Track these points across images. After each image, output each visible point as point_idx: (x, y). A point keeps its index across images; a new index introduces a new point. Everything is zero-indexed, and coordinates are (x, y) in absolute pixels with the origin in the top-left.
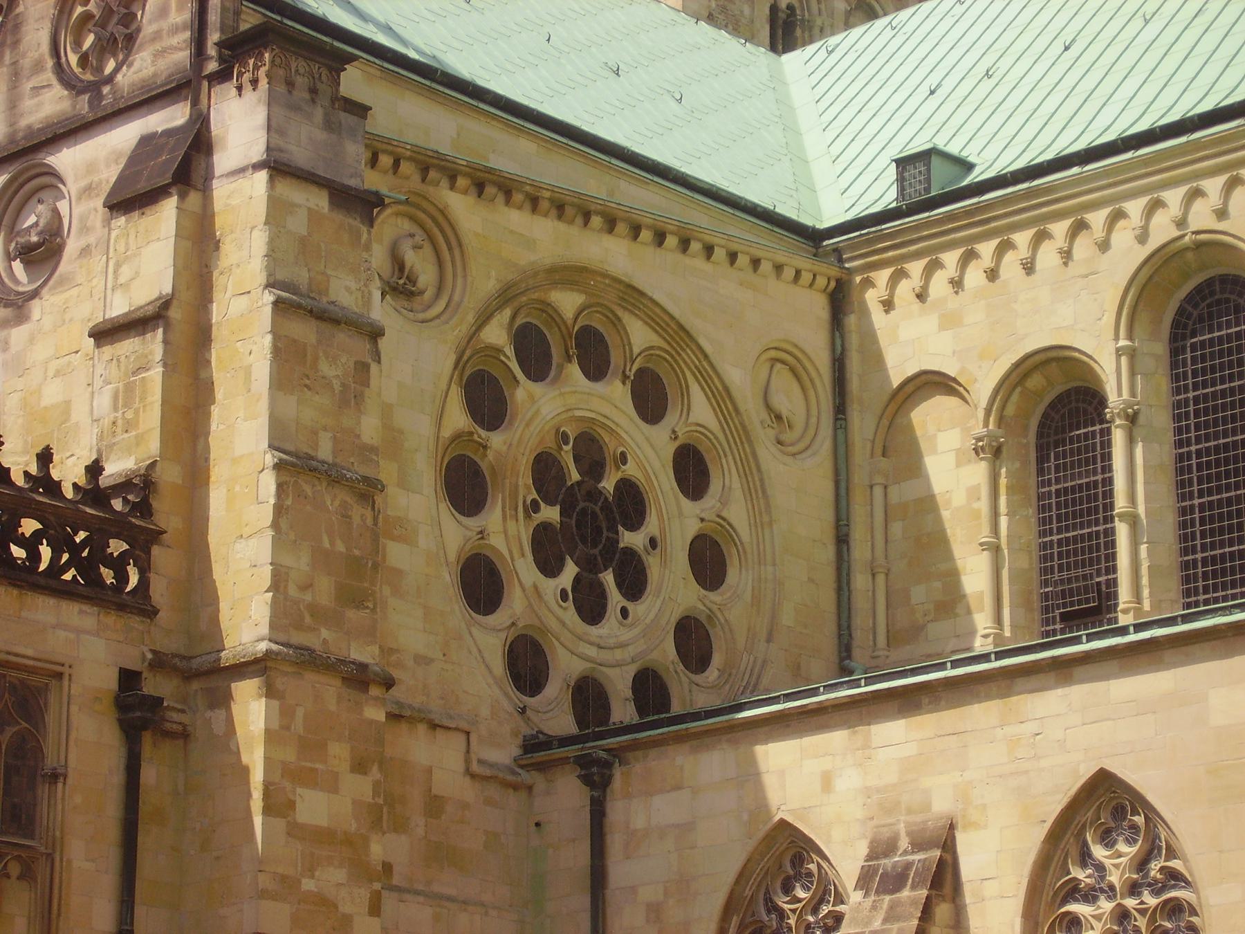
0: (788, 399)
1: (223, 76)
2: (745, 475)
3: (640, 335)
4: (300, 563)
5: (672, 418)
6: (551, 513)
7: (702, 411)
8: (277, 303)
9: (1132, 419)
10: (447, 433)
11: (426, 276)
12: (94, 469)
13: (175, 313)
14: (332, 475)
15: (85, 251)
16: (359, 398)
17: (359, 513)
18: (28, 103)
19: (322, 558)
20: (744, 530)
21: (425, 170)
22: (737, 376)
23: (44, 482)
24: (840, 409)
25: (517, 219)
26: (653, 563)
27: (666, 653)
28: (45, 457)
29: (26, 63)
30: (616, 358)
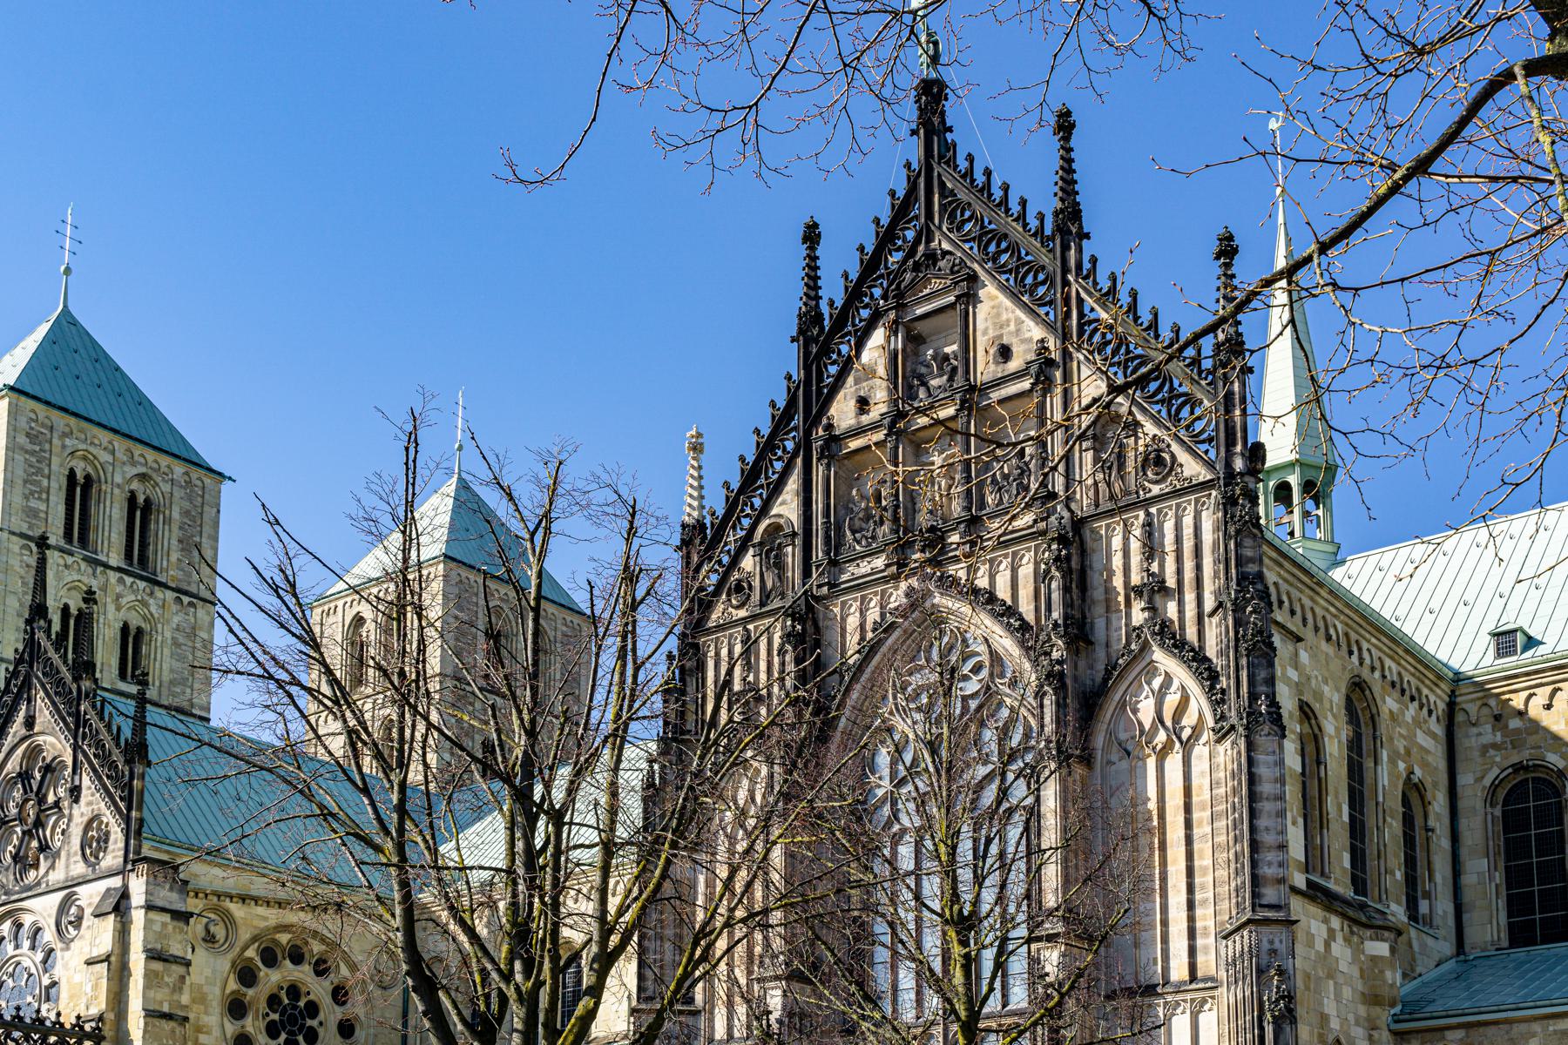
1: (133, 870)
10: (228, 991)
13: (113, 959)
15: (89, 927)
16: (181, 989)
18: (72, 867)
21: (219, 896)
29: (72, 851)
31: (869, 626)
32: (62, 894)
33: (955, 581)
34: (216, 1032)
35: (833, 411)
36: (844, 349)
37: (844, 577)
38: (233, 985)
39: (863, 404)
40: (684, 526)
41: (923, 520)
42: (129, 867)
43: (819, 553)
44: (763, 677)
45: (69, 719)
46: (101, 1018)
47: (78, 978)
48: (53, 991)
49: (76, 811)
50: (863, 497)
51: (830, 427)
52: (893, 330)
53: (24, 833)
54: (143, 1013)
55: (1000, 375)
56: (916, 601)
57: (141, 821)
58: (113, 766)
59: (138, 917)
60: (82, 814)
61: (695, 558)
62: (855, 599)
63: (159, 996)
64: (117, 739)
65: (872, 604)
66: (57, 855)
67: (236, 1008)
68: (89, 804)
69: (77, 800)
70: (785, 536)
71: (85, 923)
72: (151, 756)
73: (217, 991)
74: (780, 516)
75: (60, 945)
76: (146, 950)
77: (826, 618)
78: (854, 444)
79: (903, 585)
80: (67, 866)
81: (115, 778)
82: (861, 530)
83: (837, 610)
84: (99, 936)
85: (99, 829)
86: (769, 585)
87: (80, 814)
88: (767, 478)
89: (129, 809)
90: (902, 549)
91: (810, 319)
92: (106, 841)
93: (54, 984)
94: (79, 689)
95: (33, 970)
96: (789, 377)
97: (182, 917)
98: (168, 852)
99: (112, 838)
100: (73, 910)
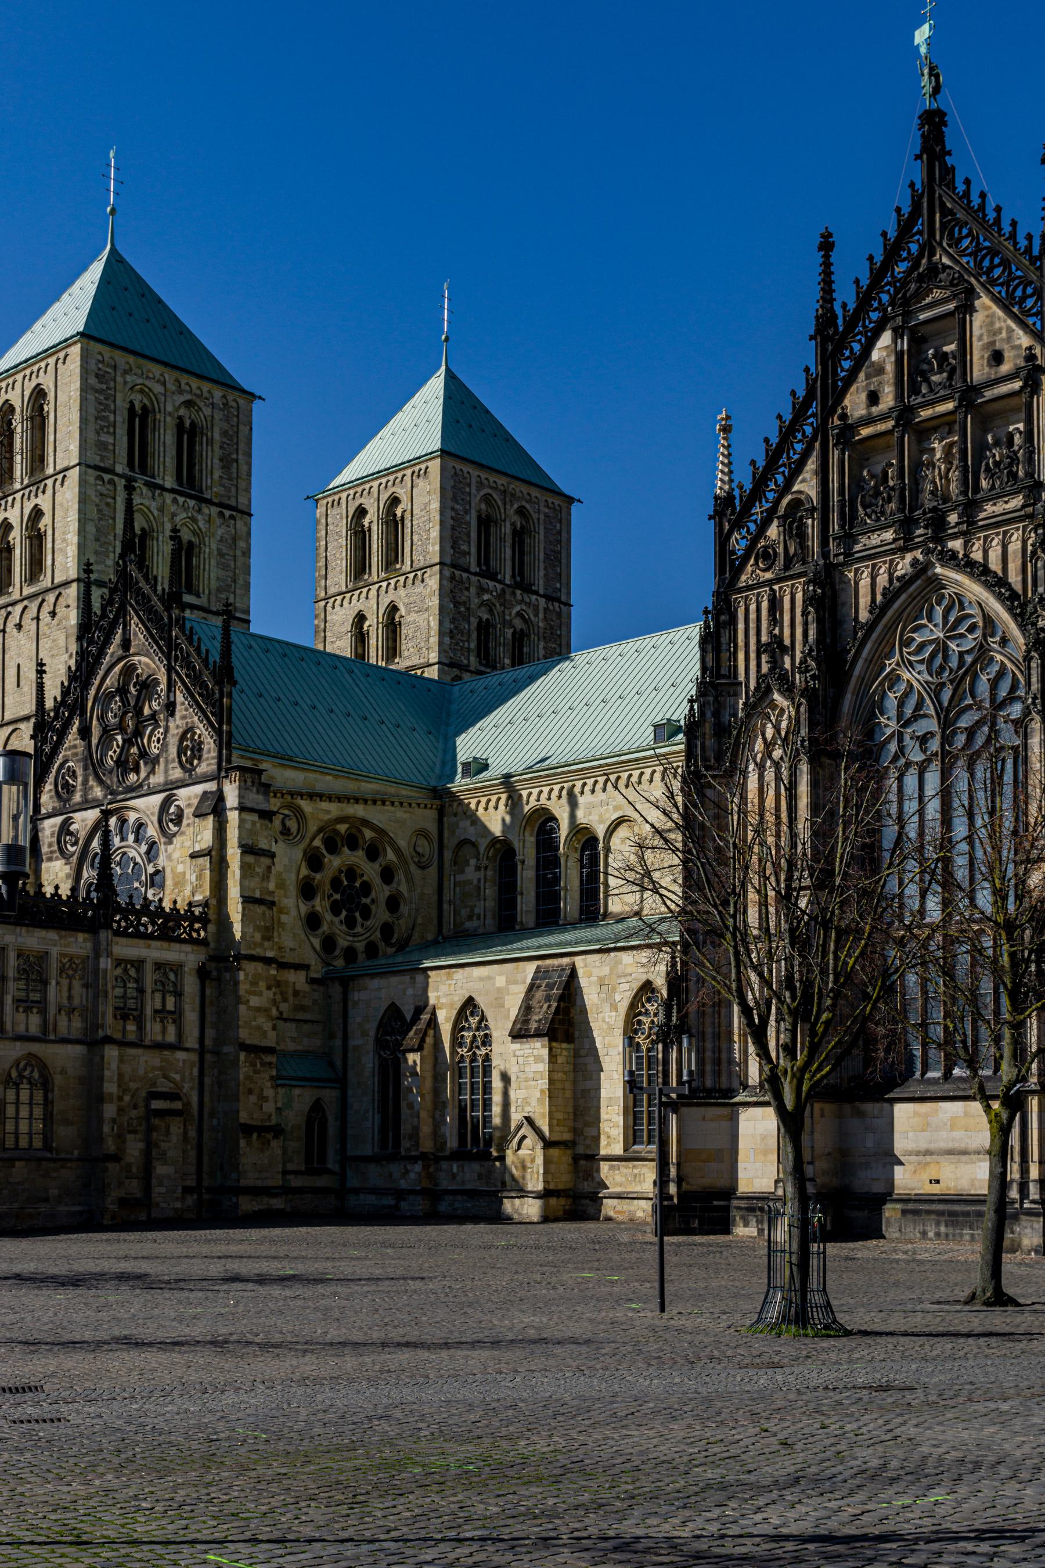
12: (190, 904)
15: (188, 825)
23: (175, 909)
28: (175, 902)
31: (879, 590)
32: (162, 796)
33: (954, 555)
34: (294, 912)
35: (846, 402)
36: (857, 347)
37: (858, 547)
38: (304, 871)
39: (873, 398)
40: (717, 498)
41: (928, 501)
42: (223, 774)
43: (835, 527)
44: (787, 632)
45: (162, 643)
47: (180, 868)
48: (157, 878)
50: (872, 476)
51: (844, 417)
52: (897, 333)
53: (124, 741)
55: (993, 377)
56: (921, 570)
57: (230, 734)
58: (203, 685)
59: (233, 817)
60: (178, 727)
61: (727, 527)
62: (867, 567)
64: (205, 662)
65: (882, 571)
66: (155, 761)
67: (307, 891)
68: (183, 717)
69: (172, 714)
70: (805, 510)
71: (185, 822)
72: (236, 675)
74: (800, 492)
75: (163, 840)
76: (241, 846)
77: (842, 582)
78: (865, 432)
79: (909, 557)
80: (166, 771)
81: (207, 696)
82: (870, 505)
83: (851, 575)
84: (204, 834)
85: (192, 739)
86: (792, 551)
87: (176, 725)
88: (789, 458)
90: (906, 527)
91: (825, 321)
92: (200, 750)
93: (157, 872)
94: (170, 617)
95: (138, 860)
96: (807, 370)
97: (266, 815)
98: (251, 759)
99: (205, 747)
100: (172, 810)
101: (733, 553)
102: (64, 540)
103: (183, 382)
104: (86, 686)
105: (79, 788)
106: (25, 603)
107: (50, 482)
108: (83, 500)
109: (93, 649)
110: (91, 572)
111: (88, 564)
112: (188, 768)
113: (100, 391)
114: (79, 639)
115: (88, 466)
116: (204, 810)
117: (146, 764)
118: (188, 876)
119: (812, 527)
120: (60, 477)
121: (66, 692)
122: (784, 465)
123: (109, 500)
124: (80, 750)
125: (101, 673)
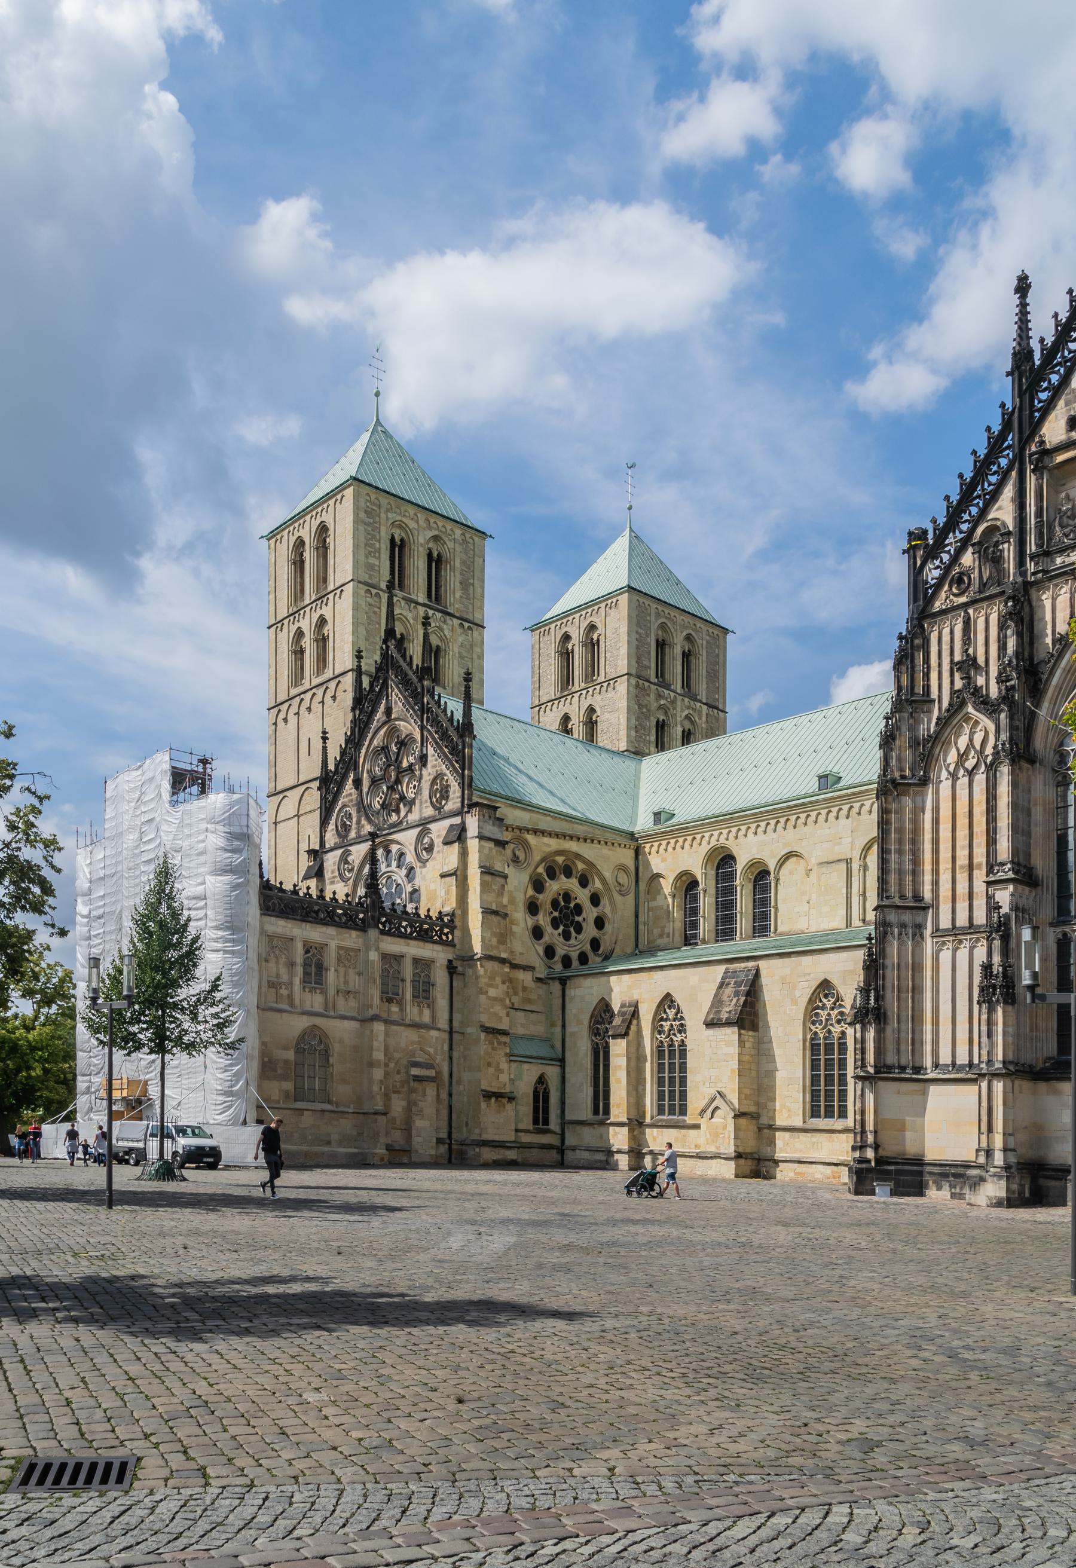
0: (623, 879)
1: (468, 812)
2: (610, 901)
3: (580, 866)
4: (488, 935)
5: (590, 887)
6: (556, 914)
7: (598, 884)
8: (482, 873)
9: (705, 891)
11: (522, 857)
14: (495, 913)
16: (502, 894)
17: (502, 922)
19: (494, 934)
20: (609, 915)
21: (520, 830)
22: (607, 875)
24: (637, 881)
25: (546, 840)
26: (584, 925)
27: (587, 948)
30: (574, 872)
32: (419, 829)
42: (466, 809)
46: (452, 915)
47: (432, 887)
48: (415, 896)
49: (425, 772)
53: (388, 788)
54: (481, 910)
59: (473, 845)
63: (490, 899)
66: (412, 802)
71: (436, 849)
73: (522, 896)
75: (419, 864)
80: (421, 810)
81: (454, 750)
84: (447, 858)
89: (463, 769)
97: (501, 844)
98: (488, 799)
100: (425, 841)
101: (927, 582)
102: (342, 640)
103: (432, 521)
104: (358, 746)
105: (354, 826)
106: (314, 690)
107: (331, 596)
108: (356, 608)
109: (365, 718)
110: (362, 657)
111: (359, 651)
112: (438, 808)
113: (369, 524)
114: (353, 709)
115: (359, 582)
116: (451, 839)
117: (405, 805)
118: (438, 893)
119: (1009, 551)
120: (338, 591)
121: (343, 753)
122: (979, 497)
123: (376, 610)
124: (354, 797)
125: (370, 735)
